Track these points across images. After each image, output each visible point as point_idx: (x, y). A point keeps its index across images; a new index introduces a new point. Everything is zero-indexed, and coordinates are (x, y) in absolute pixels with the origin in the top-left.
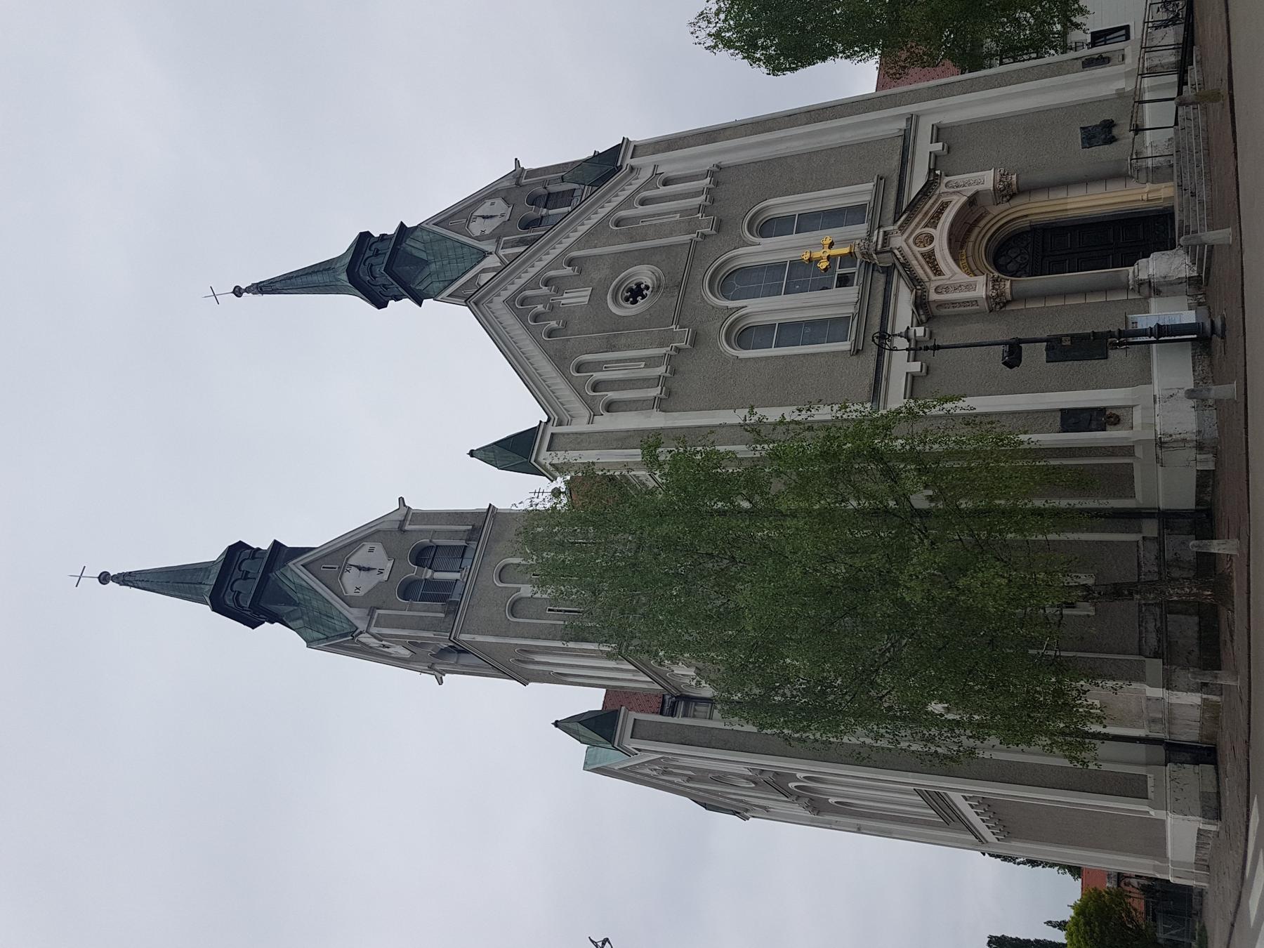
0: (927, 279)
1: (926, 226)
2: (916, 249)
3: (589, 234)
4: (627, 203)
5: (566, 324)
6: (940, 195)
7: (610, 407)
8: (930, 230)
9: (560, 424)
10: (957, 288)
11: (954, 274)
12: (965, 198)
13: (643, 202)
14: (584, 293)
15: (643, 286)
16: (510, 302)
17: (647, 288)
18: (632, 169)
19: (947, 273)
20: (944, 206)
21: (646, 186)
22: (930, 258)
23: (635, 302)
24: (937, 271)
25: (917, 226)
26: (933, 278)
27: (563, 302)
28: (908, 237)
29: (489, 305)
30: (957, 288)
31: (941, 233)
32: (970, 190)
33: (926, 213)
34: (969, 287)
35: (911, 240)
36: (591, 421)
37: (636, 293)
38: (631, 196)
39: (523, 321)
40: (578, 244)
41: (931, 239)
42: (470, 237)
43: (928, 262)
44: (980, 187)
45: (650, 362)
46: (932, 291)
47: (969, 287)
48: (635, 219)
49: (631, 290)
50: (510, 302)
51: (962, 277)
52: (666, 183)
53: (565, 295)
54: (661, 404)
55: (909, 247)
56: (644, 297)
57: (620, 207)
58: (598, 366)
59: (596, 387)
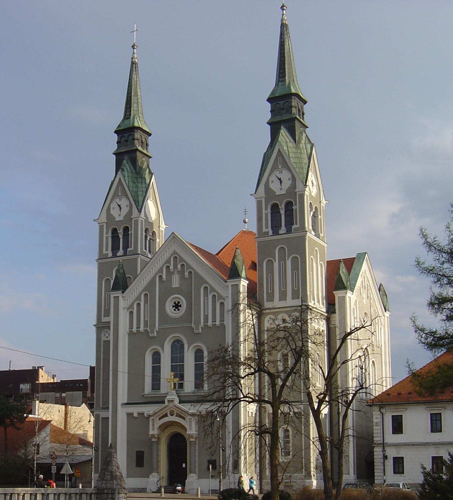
0: (157, 415)
1: (177, 413)
2: (169, 410)
3: (200, 277)
4: (213, 290)
5: (163, 282)
6: (186, 416)
7: (131, 313)
8: (175, 414)
9: (123, 297)
10: (153, 425)
11: (158, 424)
12: (184, 424)
13: (214, 296)
14: (177, 284)
15: (179, 308)
16: (175, 252)
17: (179, 310)
18: (228, 286)
19: (158, 422)
20: (184, 418)
21: (221, 297)
22: (166, 415)
23: (173, 307)
24: (160, 419)
25: (176, 410)
26: (158, 418)
27: (175, 276)
28: (173, 408)
29: (175, 243)
30: (153, 425)
31: (174, 418)
32: (187, 426)
33: (181, 413)
34: (153, 429)
35: (172, 409)
36: (124, 308)
37: (177, 306)
38: (215, 291)
39: (166, 263)
40: (197, 274)
41: (172, 415)
42: (269, 176)
43: (164, 415)
44: (188, 430)
45: (146, 323)
46: (152, 418)
47: (153, 429)
48: (206, 295)
49: (179, 302)
50: (175, 252)
51: (157, 426)
52: (222, 304)
53: (177, 275)
54: (131, 334)
55: (169, 409)
56: (175, 310)
57: (211, 286)
58: (146, 302)
59: (139, 305)
